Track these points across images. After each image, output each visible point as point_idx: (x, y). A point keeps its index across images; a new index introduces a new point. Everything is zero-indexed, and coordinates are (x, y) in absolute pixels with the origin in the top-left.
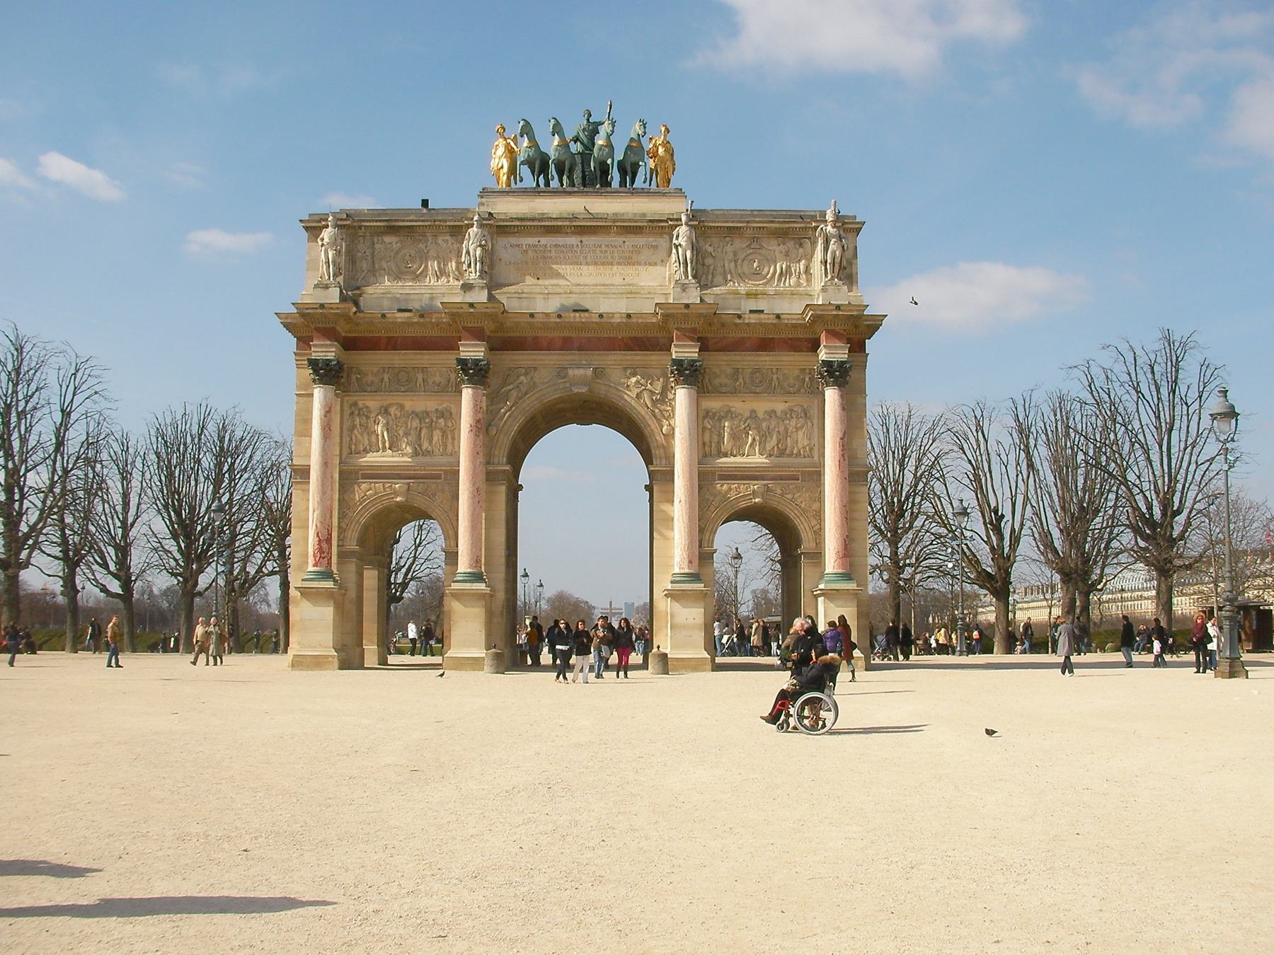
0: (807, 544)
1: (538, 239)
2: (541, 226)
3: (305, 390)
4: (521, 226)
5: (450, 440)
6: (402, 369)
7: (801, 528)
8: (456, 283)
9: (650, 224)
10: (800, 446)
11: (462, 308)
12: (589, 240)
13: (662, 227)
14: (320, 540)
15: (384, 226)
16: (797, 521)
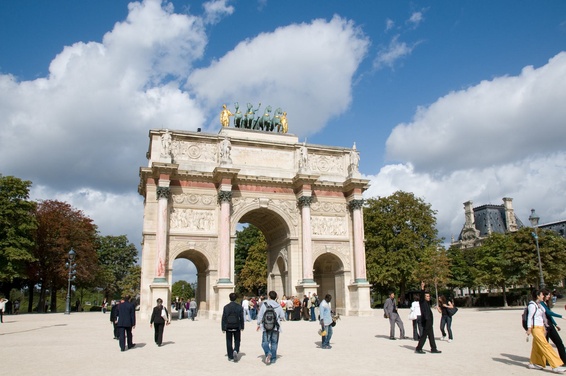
0: (346, 268)
1: (245, 148)
2: (247, 143)
3: (151, 201)
4: (240, 142)
5: (212, 224)
6: (193, 195)
7: (343, 262)
8: (214, 162)
9: (288, 146)
10: (341, 232)
11: (224, 170)
12: (265, 150)
13: (292, 147)
14: (161, 265)
15: (185, 136)
16: (342, 259)
